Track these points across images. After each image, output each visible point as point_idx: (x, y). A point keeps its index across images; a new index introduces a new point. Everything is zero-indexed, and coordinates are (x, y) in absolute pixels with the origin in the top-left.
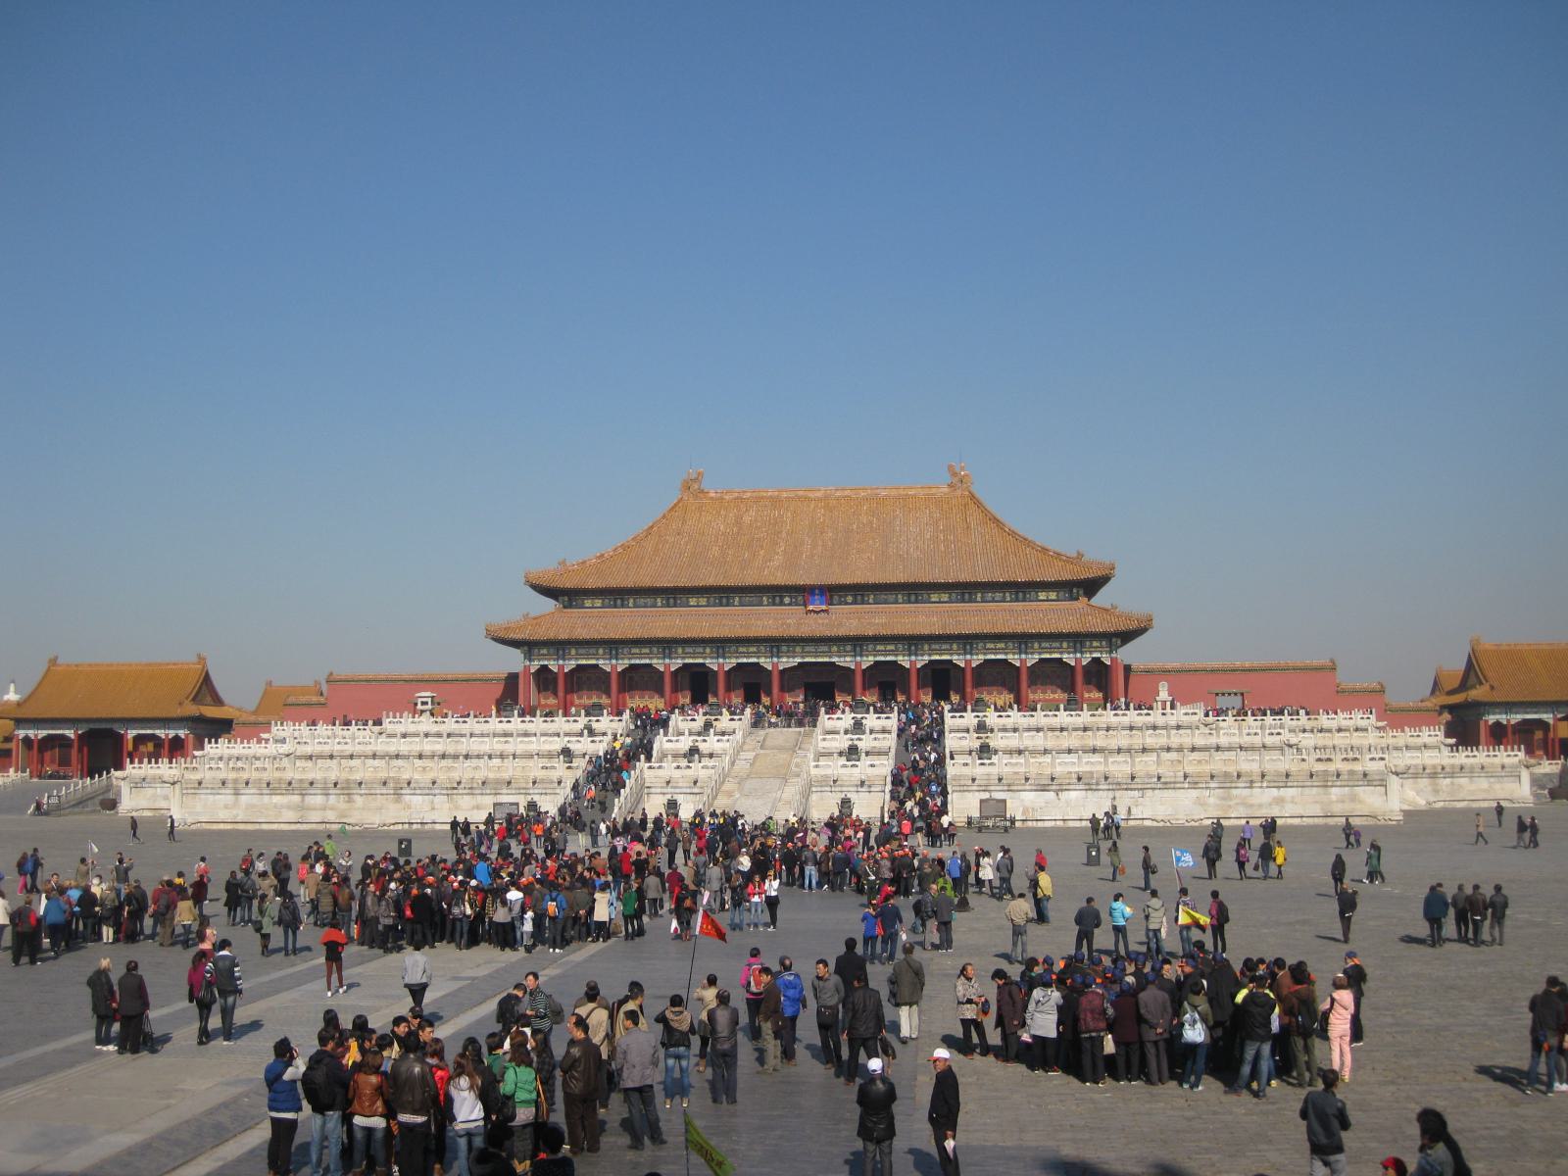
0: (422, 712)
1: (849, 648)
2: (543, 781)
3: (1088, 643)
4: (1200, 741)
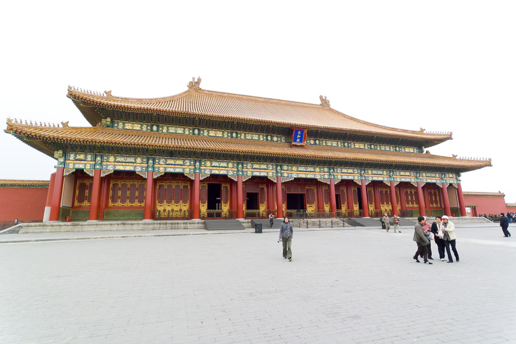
3: (447, 175)
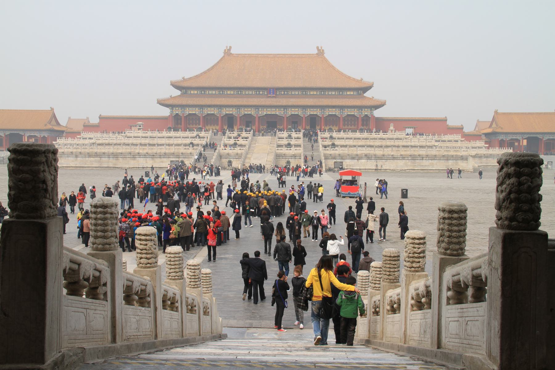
0: (139, 129)
1: (282, 109)
2: (184, 154)
4: (405, 144)
